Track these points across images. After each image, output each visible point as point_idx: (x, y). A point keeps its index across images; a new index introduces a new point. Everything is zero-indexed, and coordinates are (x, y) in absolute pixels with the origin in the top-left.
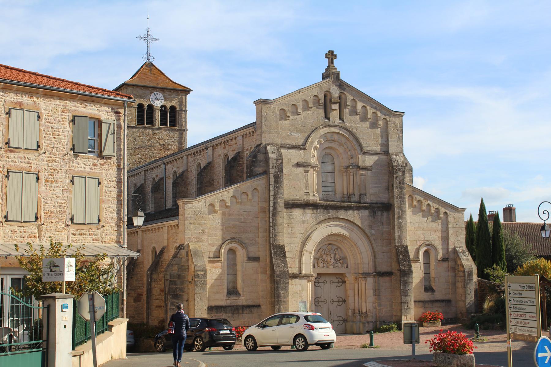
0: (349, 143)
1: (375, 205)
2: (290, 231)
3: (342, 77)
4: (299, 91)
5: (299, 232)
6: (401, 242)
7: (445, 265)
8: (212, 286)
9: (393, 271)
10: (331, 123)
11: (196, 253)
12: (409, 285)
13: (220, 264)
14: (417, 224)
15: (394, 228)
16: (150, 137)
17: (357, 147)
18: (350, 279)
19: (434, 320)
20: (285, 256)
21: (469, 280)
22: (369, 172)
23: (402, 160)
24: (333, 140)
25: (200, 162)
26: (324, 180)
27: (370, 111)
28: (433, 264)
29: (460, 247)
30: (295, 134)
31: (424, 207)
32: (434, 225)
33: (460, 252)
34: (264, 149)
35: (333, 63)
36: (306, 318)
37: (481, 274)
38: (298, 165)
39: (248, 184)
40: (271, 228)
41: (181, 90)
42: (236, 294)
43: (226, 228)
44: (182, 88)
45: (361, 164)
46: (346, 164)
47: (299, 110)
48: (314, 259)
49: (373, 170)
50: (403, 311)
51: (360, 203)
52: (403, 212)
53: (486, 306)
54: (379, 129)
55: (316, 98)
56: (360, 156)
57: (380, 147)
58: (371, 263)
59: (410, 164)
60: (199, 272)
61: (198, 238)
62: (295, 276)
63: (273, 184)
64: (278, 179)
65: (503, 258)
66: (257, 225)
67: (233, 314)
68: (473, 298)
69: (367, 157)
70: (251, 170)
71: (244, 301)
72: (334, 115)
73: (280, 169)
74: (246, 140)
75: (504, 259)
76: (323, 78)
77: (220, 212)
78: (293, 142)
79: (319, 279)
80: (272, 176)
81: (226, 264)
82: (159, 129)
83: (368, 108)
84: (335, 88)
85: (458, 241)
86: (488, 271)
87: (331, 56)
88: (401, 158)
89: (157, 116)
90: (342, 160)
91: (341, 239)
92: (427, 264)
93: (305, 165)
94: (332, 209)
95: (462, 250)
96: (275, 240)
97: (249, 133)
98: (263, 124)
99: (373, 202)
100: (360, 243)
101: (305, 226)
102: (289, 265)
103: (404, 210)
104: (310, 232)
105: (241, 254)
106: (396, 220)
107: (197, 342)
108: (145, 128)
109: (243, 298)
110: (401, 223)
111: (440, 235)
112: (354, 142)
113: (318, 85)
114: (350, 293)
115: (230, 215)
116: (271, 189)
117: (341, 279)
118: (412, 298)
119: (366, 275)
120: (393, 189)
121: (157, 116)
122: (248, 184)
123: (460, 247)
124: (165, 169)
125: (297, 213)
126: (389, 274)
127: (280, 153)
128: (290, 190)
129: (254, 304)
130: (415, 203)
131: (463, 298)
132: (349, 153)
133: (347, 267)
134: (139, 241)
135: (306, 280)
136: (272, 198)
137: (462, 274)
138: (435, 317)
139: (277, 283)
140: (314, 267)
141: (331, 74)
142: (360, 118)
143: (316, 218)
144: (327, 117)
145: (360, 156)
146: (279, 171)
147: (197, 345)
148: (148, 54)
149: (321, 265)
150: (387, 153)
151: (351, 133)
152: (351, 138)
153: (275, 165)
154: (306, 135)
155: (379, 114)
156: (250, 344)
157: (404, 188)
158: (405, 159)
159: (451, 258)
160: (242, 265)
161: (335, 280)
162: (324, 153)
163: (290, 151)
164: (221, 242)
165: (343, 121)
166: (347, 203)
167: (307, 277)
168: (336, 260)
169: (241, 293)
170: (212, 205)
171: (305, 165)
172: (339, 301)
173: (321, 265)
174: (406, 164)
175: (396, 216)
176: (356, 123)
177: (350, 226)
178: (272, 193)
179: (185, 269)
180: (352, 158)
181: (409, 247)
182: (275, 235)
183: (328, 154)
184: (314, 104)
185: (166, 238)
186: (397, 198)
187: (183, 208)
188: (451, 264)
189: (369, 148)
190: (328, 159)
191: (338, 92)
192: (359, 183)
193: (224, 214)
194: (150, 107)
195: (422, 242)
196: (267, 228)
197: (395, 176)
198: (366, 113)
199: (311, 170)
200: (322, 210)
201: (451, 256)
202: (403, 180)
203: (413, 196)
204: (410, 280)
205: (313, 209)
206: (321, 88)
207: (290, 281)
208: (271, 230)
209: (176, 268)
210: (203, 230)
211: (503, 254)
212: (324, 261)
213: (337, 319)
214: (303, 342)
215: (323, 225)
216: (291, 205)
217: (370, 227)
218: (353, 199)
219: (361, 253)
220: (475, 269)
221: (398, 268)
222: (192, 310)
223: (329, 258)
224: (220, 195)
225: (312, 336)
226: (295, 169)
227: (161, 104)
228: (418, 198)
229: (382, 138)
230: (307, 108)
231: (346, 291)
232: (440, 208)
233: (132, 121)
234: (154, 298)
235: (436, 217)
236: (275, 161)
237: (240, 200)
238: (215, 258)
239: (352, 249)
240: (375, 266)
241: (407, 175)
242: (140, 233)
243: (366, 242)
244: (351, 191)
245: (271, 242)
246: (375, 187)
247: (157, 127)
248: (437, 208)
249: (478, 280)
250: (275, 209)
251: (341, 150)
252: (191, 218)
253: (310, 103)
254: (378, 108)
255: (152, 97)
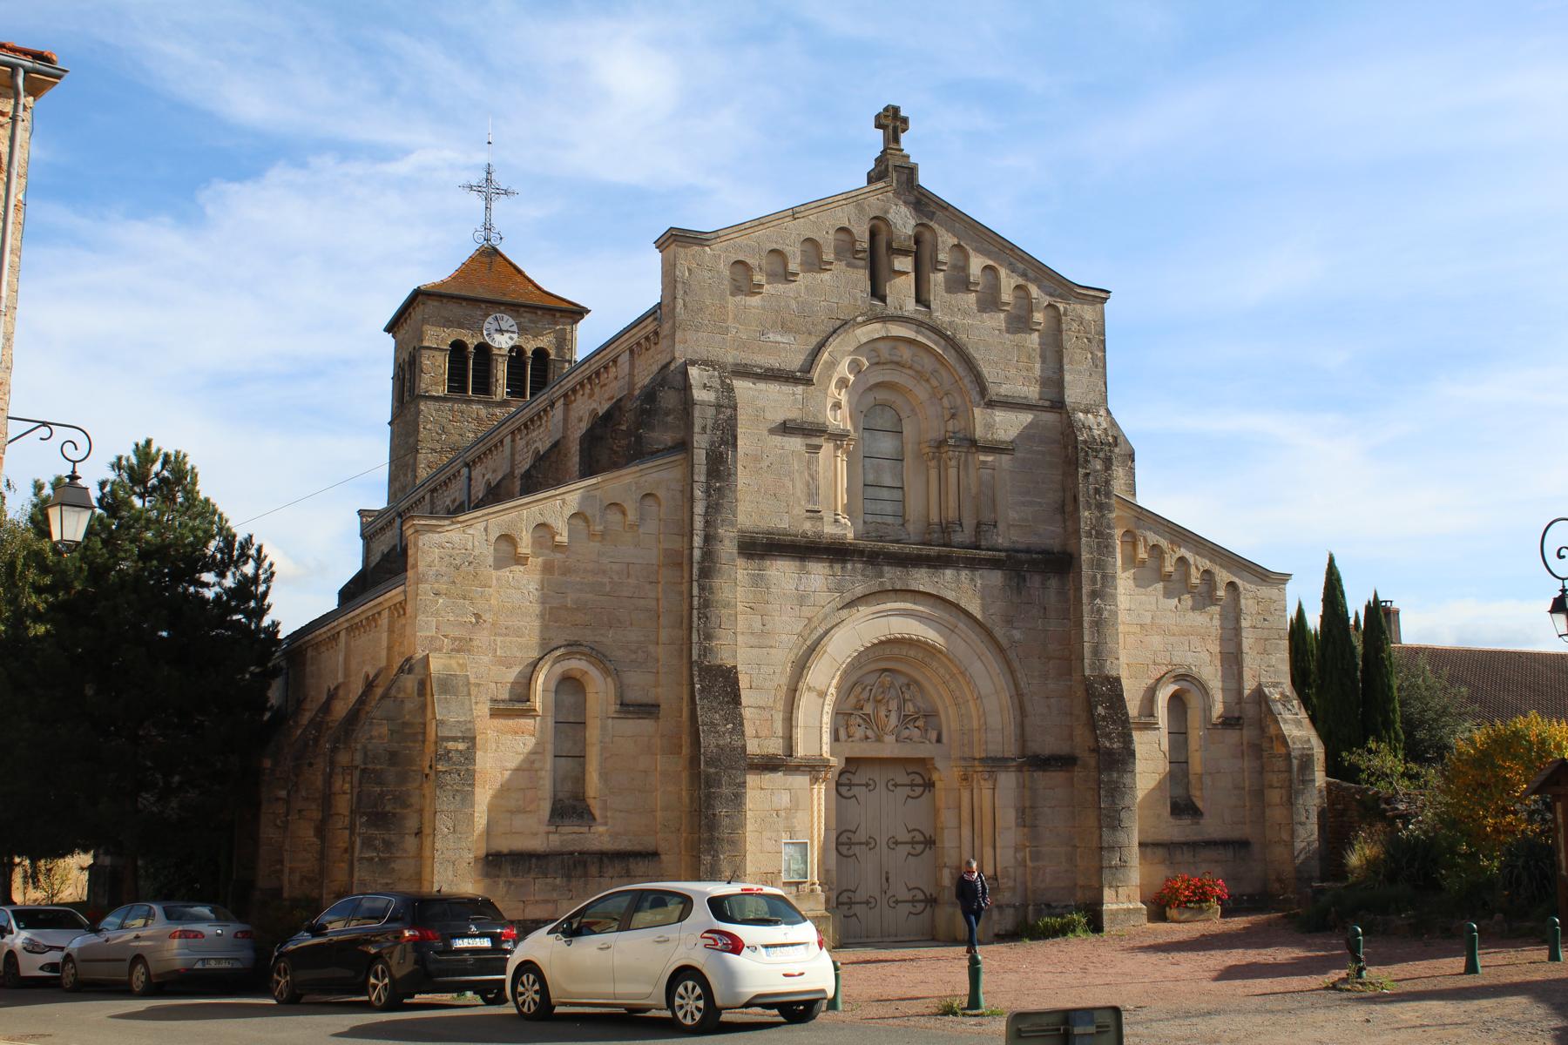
0: (943, 372)
1: (1023, 556)
2: (757, 626)
3: (925, 180)
4: (794, 213)
5: (787, 629)
6: (1102, 667)
7: (1232, 736)
8: (504, 790)
9: (1078, 752)
10: (890, 311)
11: (447, 685)
12: (1123, 794)
13: (532, 721)
14: (1149, 615)
15: (1079, 624)
16: (480, 424)
17: (969, 386)
18: (946, 775)
19: (1200, 901)
20: (735, 699)
21: (1304, 782)
22: (1005, 458)
23: (1104, 425)
24: (897, 363)
25: (539, 444)
26: (871, 478)
27: (1008, 282)
28: (1196, 734)
29: (1275, 685)
30: (779, 338)
31: (1169, 567)
32: (1199, 619)
33: (1275, 701)
34: (679, 377)
35: (896, 140)
36: (718, 906)
37: (1333, 768)
38: (786, 428)
39: (628, 480)
40: (695, 612)
41: (561, 311)
42: (581, 816)
43: (552, 613)
44: (565, 305)
45: (979, 433)
46: (935, 434)
47: (793, 266)
48: (838, 713)
49: (1018, 455)
50: (1106, 873)
51: (978, 547)
52: (1108, 579)
53: (1354, 860)
54: (1035, 336)
55: (842, 236)
56: (977, 411)
57: (1037, 388)
58: (1011, 729)
59: (1126, 441)
60: (451, 745)
61: (461, 640)
62: (769, 765)
63: (703, 479)
64: (719, 467)
65: (1394, 722)
66: (654, 603)
67: (569, 877)
68: (1316, 836)
69: (1000, 416)
70: (639, 438)
71: (606, 838)
72: (901, 290)
73: (727, 435)
74: (640, 362)
75: (1398, 726)
76: (870, 181)
77: (536, 562)
78: (773, 361)
79: (850, 776)
80: (700, 456)
81: (550, 722)
82: (504, 403)
83: (1003, 272)
84: (904, 210)
85: (1270, 669)
86: (1354, 758)
87: (892, 122)
88: (1101, 419)
89: (501, 371)
90: (925, 424)
91: (920, 656)
92: (1179, 735)
93: (807, 430)
94: (890, 564)
95: (1282, 694)
96: (706, 651)
97: (647, 338)
98: (680, 302)
99: (1018, 546)
100: (977, 668)
101: (807, 611)
102: (749, 730)
103: (1110, 571)
104: (821, 631)
105: (600, 693)
106: (1085, 600)
107: (377, 978)
108: (469, 402)
109: (601, 829)
110: (1099, 611)
111: (1216, 649)
112: (961, 370)
113: (852, 198)
114: (947, 818)
115: (566, 571)
116: (698, 493)
117: (920, 774)
118: (1132, 836)
119: (995, 764)
120: (1077, 509)
121: (501, 371)
122: (628, 480)
123: (1275, 685)
124: (470, 479)
125: (782, 572)
126: (1065, 762)
127: (731, 389)
128: (756, 503)
129: (638, 848)
130: (1142, 554)
131: (1285, 836)
132: (945, 401)
133: (939, 740)
134: (341, 659)
135: (807, 778)
136: (699, 523)
137: (1280, 764)
138: (1204, 893)
139: (708, 785)
140: (836, 738)
141: (893, 171)
142: (979, 301)
143: (839, 589)
144: (877, 293)
145: (977, 411)
146: (723, 442)
147: (375, 987)
148: (488, 228)
149: (859, 733)
150: (1057, 404)
151: (951, 342)
152: (950, 357)
153: (710, 423)
154: (814, 341)
155: (1034, 291)
156: (530, 995)
157: (1109, 508)
158: (1114, 424)
159: (1249, 718)
160: (604, 728)
161: (902, 778)
162: (870, 399)
163: (762, 386)
164: (535, 655)
165: (928, 307)
166: (939, 550)
167: (813, 768)
168: (906, 720)
169: (597, 813)
170: (508, 539)
171: (807, 430)
172: (913, 843)
173: (859, 733)
174: (1115, 438)
175: (1086, 589)
176: (966, 313)
177: (946, 616)
178: (699, 508)
179: (415, 734)
180: (953, 416)
181: (1124, 682)
182: (708, 637)
183: (883, 405)
184: (839, 254)
185: (384, 644)
186: (1089, 535)
187: (416, 545)
188: (1248, 734)
189: (1005, 390)
190: (884, 420)
191: (913, 223)
192: (974, 491)
193: (547, 568)
194: (484, 350)
195: (1165, 669)
196: (685, 613)
197: (1081, 471)
198: (995, 287)
199: (827, 447)
200: (859, 566)
201: (1250, 711)
202: (1107, 483)
203: (1138, 532)
204: (1127, 779)
205: (831, 561)
206: (860, 207)
207: (752, 780)
208: (695, 619)
209: (384, 730)
210: (478, 616)
211: (1394, 711)
212: (867, 719)
213: (908, 896)
214: (699, 998)
215: (864, 610)
216: (762, 547)
217: (1009, 621)
218: (957, 538)
219: (979, 697)
220: (1319, 751)
221: (1092, 744)
222: (429, 862)
223: (883, 713)
224: (535, 509)
225: (730, 975)
226: (778, 440)
227: (511, 343)
228: (1153, 538)
229: (1043, 362)
230: (815, 261)
231: (935, 812)
232: (1216, 570)
233: (436, 384)
234: (340, 825)
235: (1205, 596)
236: (711, 412)
237: (599, 528)
238: (515, 704)
239: (953, 685)
240: (1022, 738)
241: (1119, 472)
242: (343, 634)
243: (995, 666)
244: (952, 514)
245: (695, 657)
246: (1023, 504)
247: (498, 399)
248: (1206, 572)
249: (1328, 784)
250: (708, 555)
251: (921, 392)
252: (438, 575)
253: (824, 249)
254: (1031, 274)
255: (489, 324)
